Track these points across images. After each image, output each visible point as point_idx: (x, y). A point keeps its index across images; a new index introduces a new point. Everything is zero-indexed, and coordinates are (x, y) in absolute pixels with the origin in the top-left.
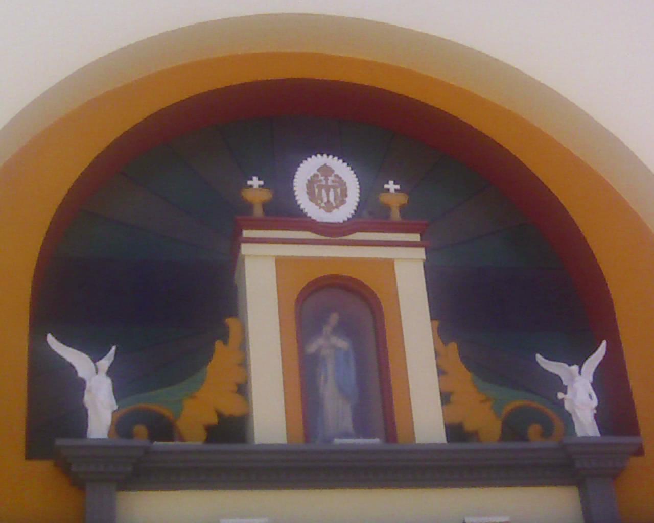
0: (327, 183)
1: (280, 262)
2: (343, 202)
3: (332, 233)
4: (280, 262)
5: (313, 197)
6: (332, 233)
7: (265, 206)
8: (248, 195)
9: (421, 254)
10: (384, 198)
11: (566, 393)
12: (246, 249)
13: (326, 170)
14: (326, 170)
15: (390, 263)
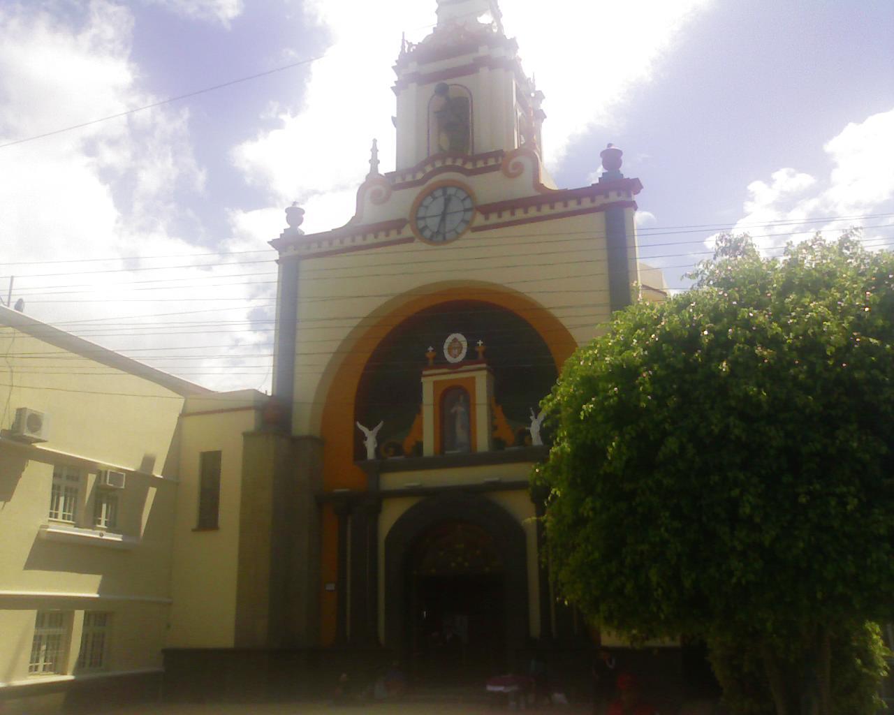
0: (456, 345)
1: (435, 383)
2: (460, 353)
3: (455, 367)
4: (435, 383)
5: (450, 353)
6: (455, 367)
7: (435, 358)
8: (428, 355)
9: (485, 373)
10: (477, 349)
11: (530, 426)
12: (423, 380)
13: (455, 340)
14: (455, 340)
15: (473, 379)
